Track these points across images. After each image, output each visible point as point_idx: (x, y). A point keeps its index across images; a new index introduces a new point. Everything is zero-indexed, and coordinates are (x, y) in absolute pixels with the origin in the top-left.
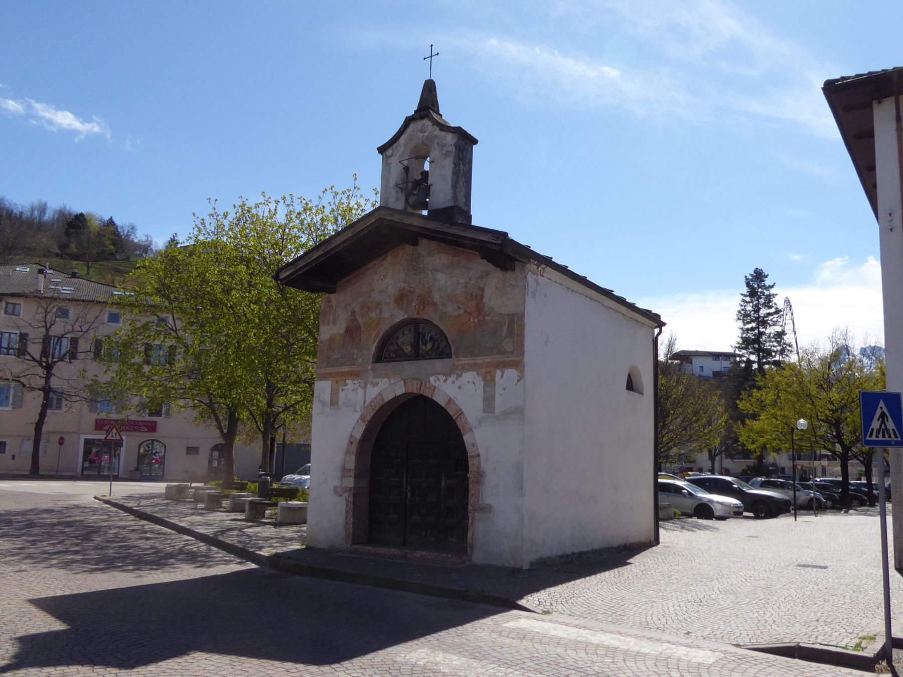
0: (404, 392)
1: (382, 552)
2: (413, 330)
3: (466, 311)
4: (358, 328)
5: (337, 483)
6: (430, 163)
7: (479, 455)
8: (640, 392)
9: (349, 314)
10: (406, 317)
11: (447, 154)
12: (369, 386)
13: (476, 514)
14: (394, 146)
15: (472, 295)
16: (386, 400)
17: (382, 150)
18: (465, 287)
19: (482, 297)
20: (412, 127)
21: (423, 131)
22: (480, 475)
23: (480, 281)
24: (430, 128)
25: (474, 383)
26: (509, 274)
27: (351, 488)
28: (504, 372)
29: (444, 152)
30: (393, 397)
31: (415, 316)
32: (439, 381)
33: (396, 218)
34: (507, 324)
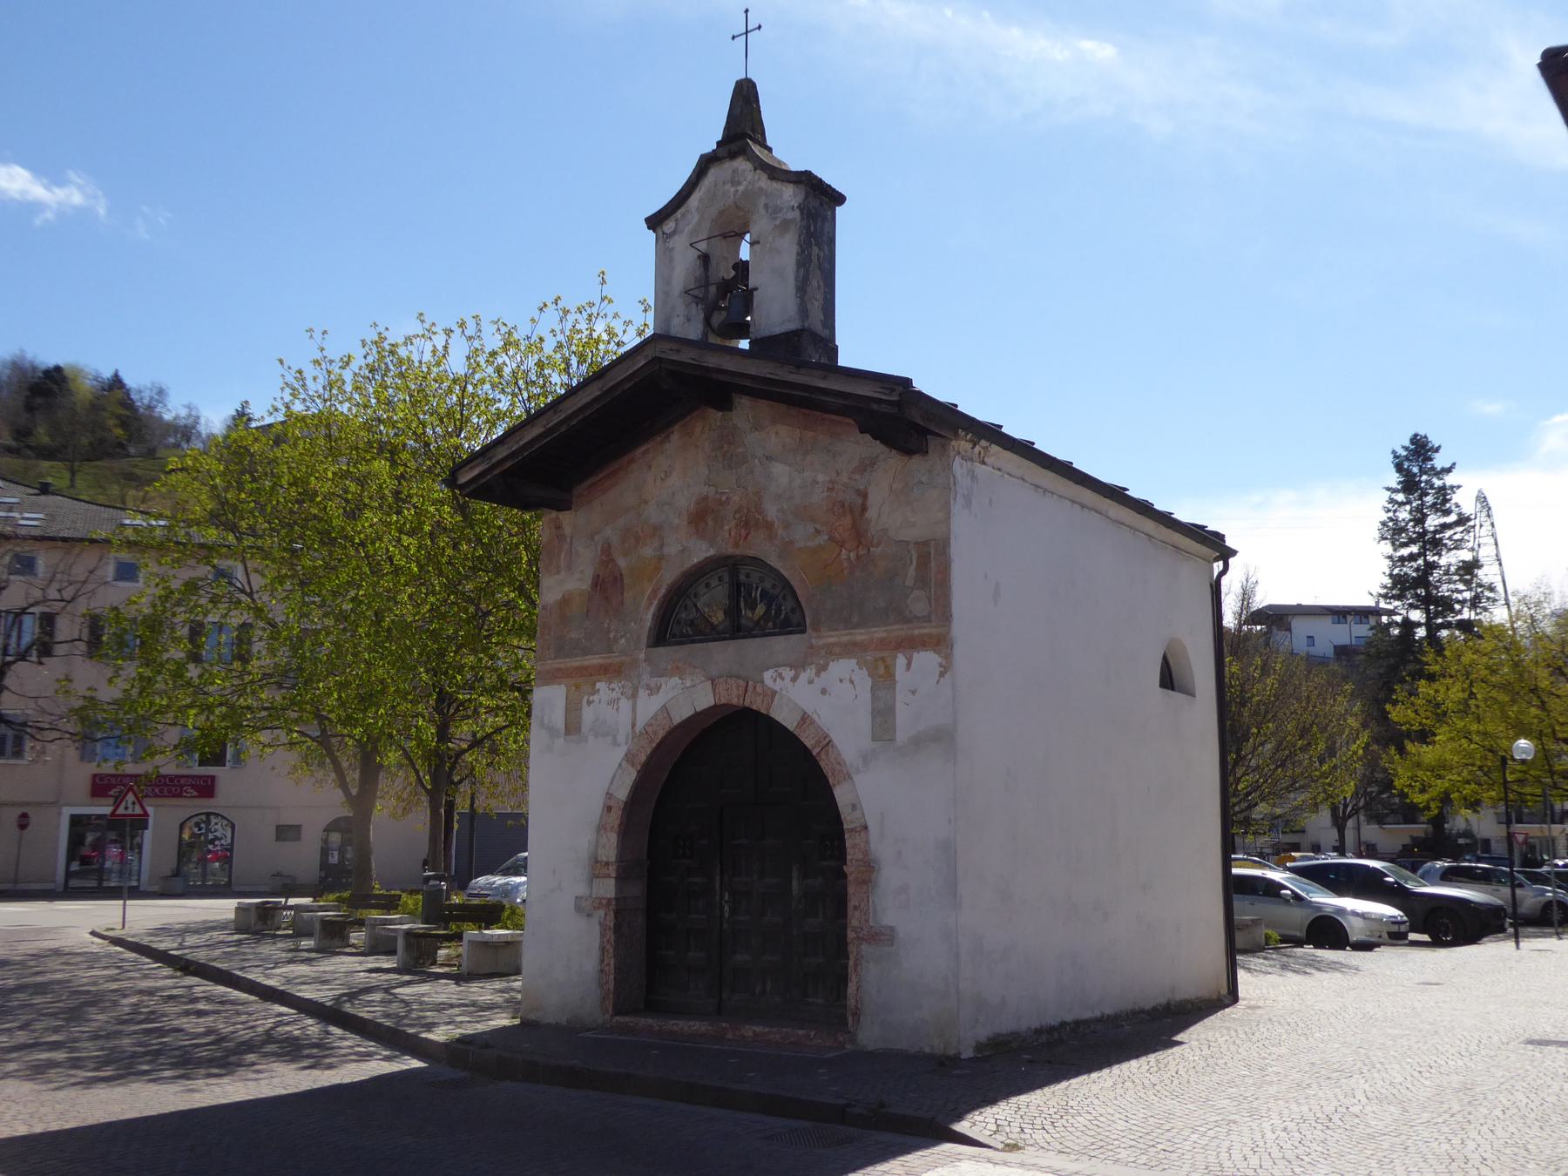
0: (712, 703)
1: (675, 1028)
2: (726, 579)
3: (831, 539)
4: (617, 579)
5: (582, 890)
6: (752, 244)
7: (866, 827)
8: (1189, 692)
9: (599, 553)
10: (712, 552)
11: (784, 227)
12: (642, 693)
13: (864, 947)
14: (679, 214)
15: (843, 506)
16: (677, 720)
17: (654, 222)
18: (830, 489)
19: (864, 509)
20: (713, 174)
21: (735, 182)
22: (870, 866)
23: (858, 477)
24: (750, 176)
25: (852, 682)
26: (916, 462)
27: (609, 900)
28: (911, 657)
29: (778, 222)
30: (692, 712)
31: (731, 551)
32: (783, 679)
33: (687, 356)
34: (914, 562)
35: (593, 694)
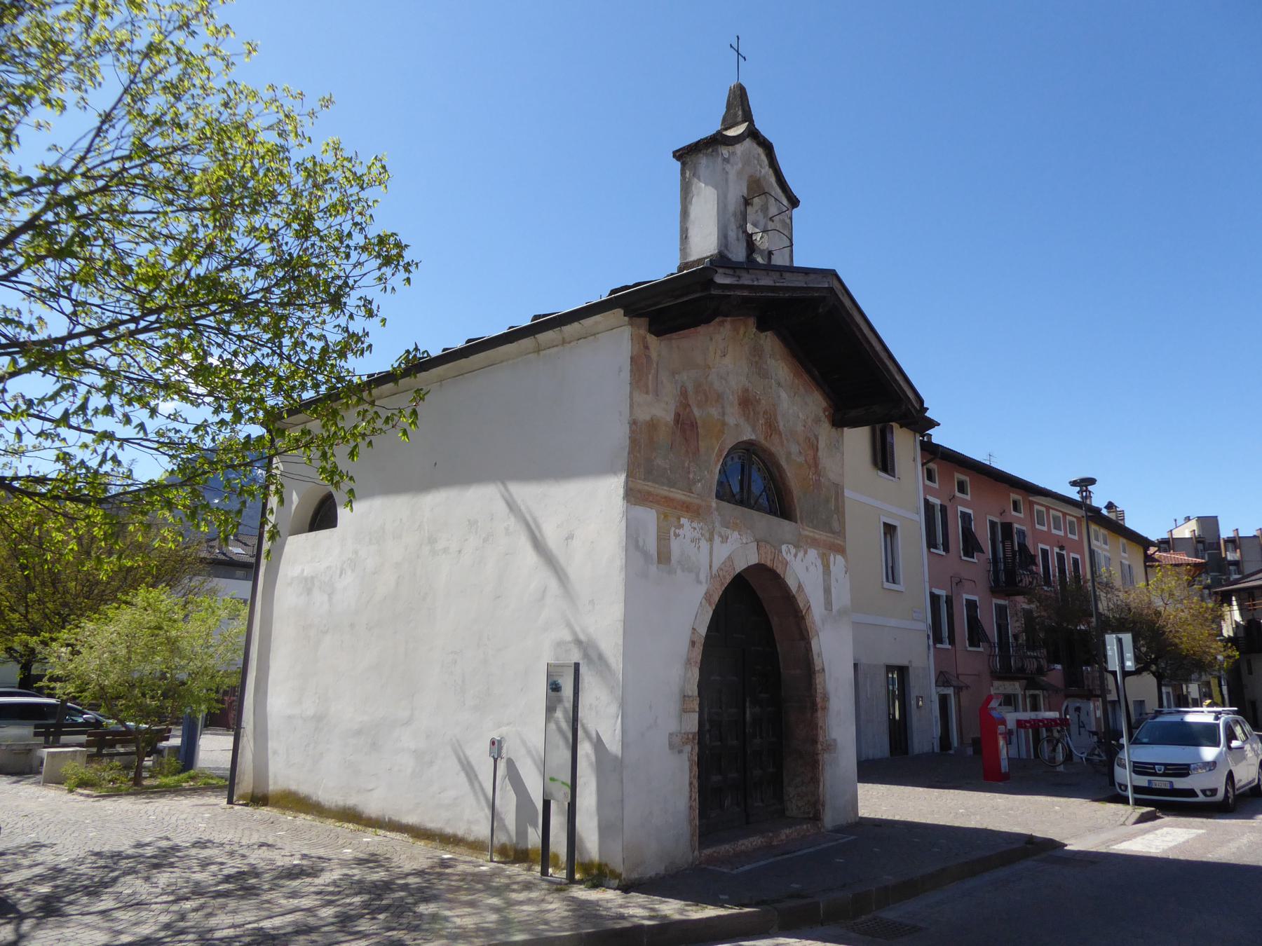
0: (757, 562)
12: (717, 539)
27: (695, 733)
35: (679, 529)
